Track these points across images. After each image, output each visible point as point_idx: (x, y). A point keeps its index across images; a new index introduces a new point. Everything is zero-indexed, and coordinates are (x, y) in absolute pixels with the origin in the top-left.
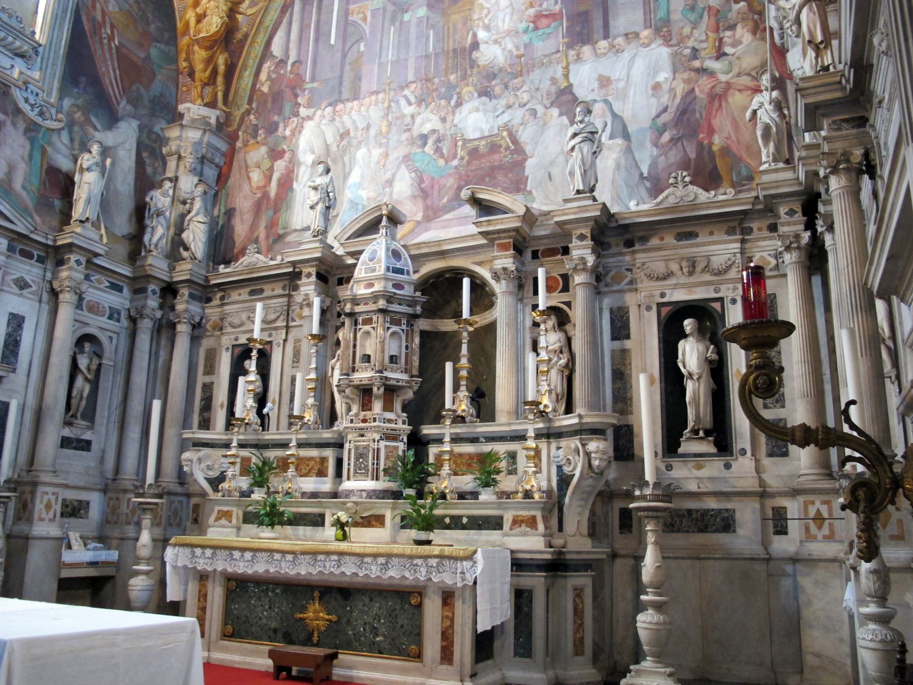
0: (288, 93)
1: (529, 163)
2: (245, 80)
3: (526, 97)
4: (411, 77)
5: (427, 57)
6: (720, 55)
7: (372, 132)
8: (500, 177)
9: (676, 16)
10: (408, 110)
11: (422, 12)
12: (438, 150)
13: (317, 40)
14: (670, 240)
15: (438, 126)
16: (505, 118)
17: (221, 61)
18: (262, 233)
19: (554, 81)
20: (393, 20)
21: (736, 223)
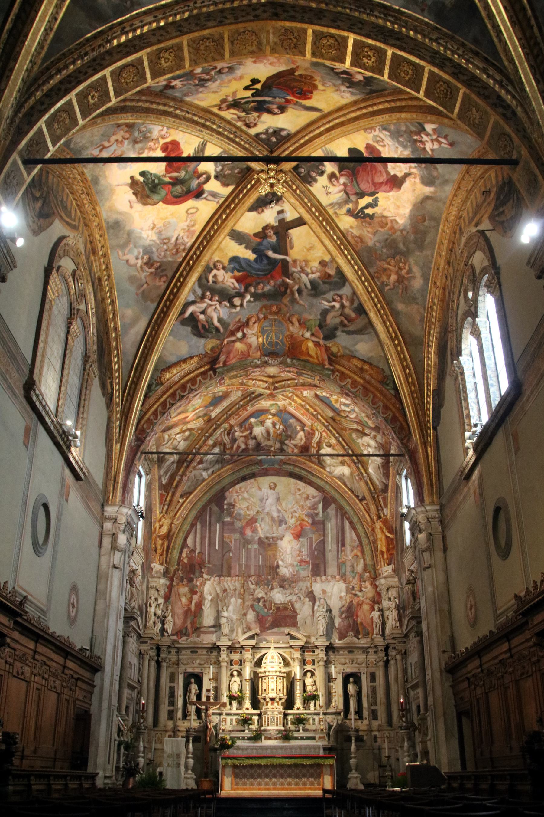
0: (197, 566)
1: (298, 617)
2: (175, 554)
3: (297, 592)
4: (253, 573)
5: (259, 566)
6: (361, 591)
7: (237, 592)
8: (288, 620)
9: (348, 573)
10: (252, 587)
11: (256, 546)
12: (264, 605)
13: (209, 545)
14: (346, 652)
15: (264, 596)
16: (289, 598)
17: (165, 545)
18: (189, 626)
19: (307, 588)
20: (244, 547)
21: (365, 650)
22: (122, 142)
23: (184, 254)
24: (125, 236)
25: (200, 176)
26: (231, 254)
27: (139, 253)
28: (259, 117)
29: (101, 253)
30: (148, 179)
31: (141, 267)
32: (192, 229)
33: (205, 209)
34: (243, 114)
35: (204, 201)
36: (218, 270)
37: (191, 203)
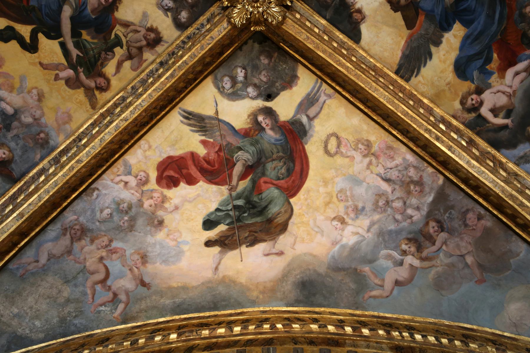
22: (114, 252)
23: (430, 170)
24: (339, 276)
25: (258, 127)
26: (450, 75)
27: (389, 257)
28: (126, 25)
29: (348, 330)
30: (228, 216)
31: (422, 259)
32: (375, 148)
33: (336, 119)
34: (119, 52)
35: (316, 122)
36: (481, 103)
37: (313, 148)
